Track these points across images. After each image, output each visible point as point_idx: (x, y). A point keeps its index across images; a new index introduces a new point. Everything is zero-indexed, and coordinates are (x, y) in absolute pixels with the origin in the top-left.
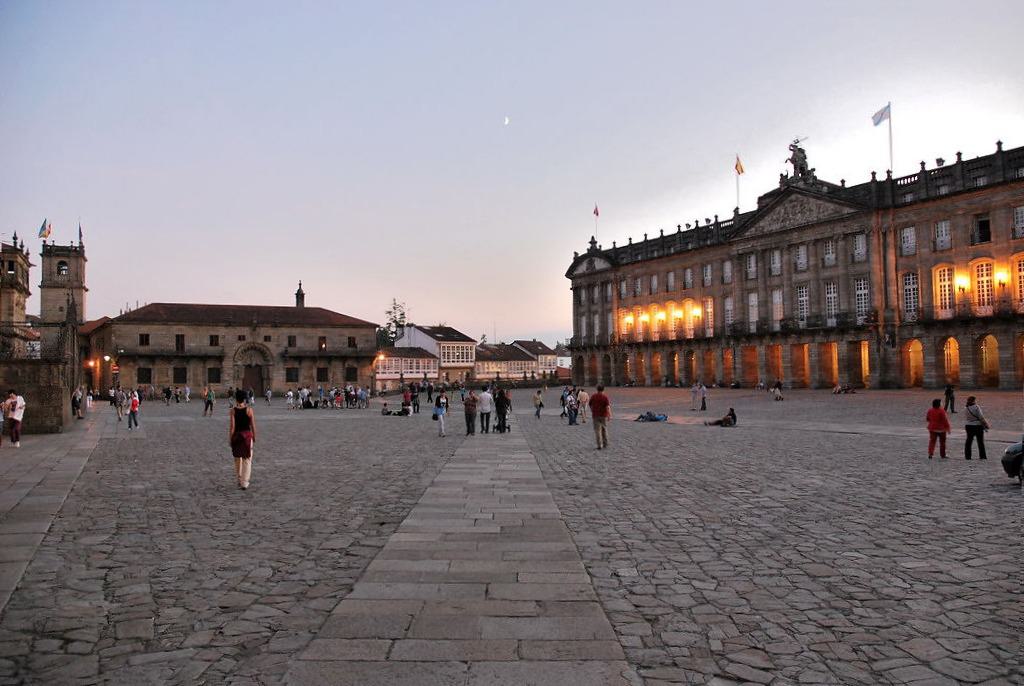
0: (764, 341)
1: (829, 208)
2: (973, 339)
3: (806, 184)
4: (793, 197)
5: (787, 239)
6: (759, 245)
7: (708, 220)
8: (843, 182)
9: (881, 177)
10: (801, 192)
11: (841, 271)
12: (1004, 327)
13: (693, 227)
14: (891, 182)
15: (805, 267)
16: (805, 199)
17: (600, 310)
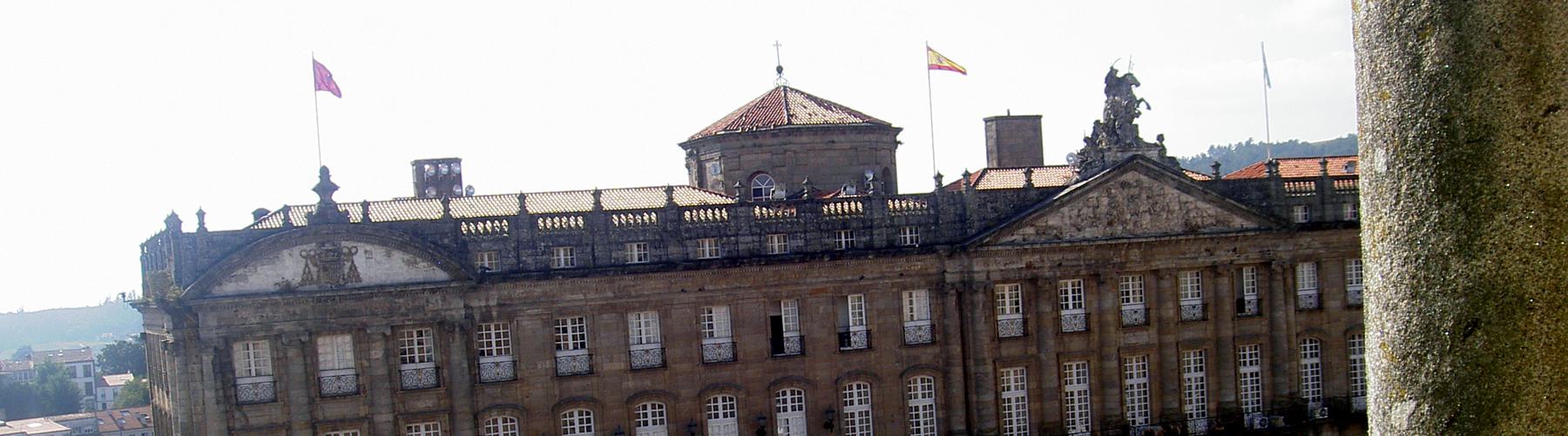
4: (1129, 177)
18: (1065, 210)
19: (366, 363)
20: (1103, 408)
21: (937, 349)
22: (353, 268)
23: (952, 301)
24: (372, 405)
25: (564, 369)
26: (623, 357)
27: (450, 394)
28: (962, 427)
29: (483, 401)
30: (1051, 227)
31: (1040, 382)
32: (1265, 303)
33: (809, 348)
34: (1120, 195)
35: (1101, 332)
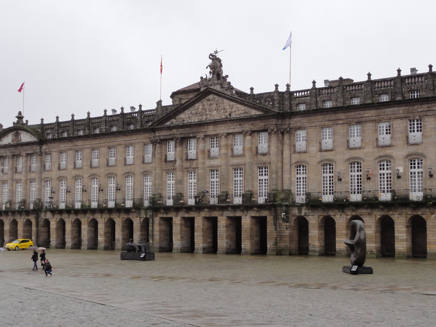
0: (180, 213)
1: (239, 110)
2: (346, 218)
3: (222, 87)
4: (211, 97)
7: (133, 108)
8: (252, 89)
9: (282, 89)
10: (218, 94)
11: (247, 159)
12: (369, 211)
13: (119, 112)
14: (290, 94)
15: (217, 154)
16: (220, 99)
17: (23, 178)
18: (186, 111)
22: (20, 138)
30: (182, 118)
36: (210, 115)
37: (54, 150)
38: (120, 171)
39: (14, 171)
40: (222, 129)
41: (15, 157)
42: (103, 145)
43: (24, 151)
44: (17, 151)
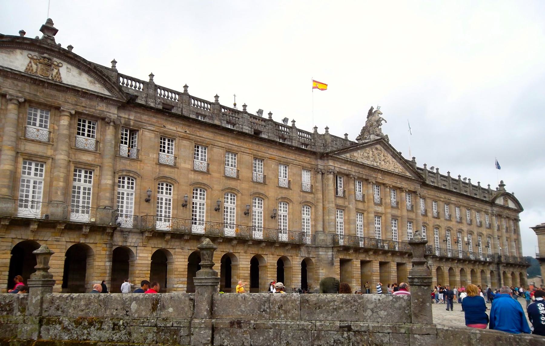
0: (360, 256)
4: (378, 146)
5: (374, 176)
6: (353, 170)
18: (359, 151)
19: (56, 127)
20: (368, 233)
21: (312, 196)
23: (319, 176)
24: (55, 150)
25: (162, 161)
26: (191, 163)
27: (101, 155)
28: (322, 229)
29: (120, 165)
30: (355, 157)
31: (349, 217)
32: (414, 207)
33: (267, 183)
34: (376, 152)
35: (368, 202)
36: (380, 163)
37: (149, 128)
38: (271, 192)
39: (20, 133)
40: (388, 180)
41: (27, 105)
42: (248, 151)
43: (68, 103)
44: (42, 95)
